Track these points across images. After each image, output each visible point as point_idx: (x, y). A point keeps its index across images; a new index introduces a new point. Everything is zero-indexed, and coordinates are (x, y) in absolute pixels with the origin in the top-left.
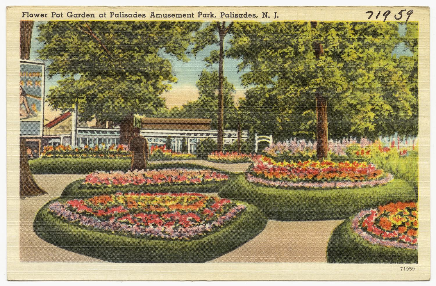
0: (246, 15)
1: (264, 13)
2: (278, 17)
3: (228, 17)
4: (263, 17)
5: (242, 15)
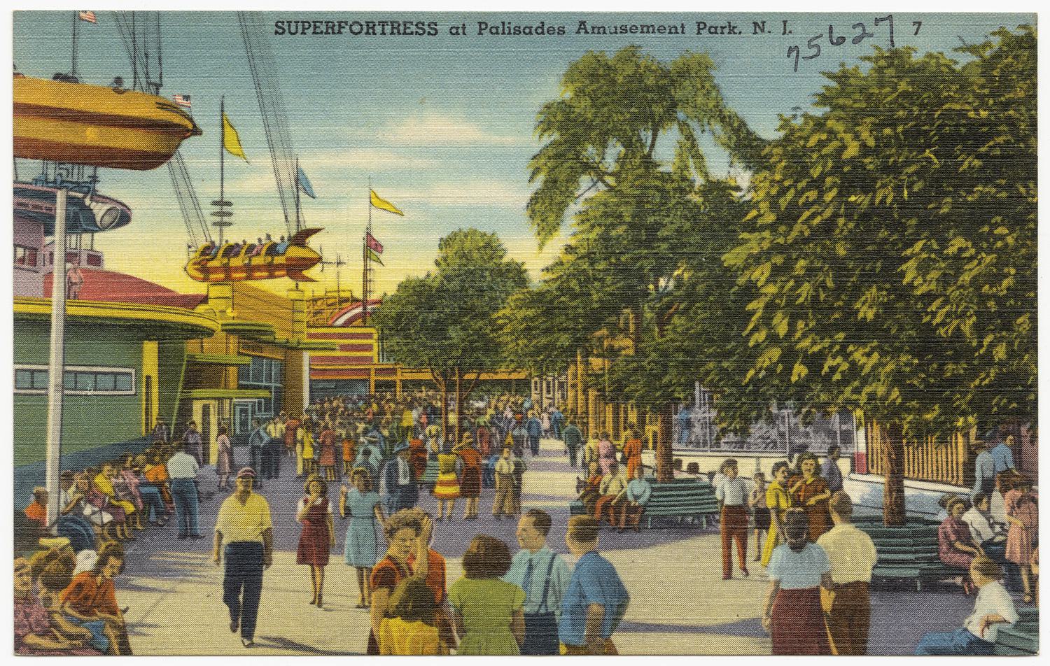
1: (756, 24)
2: (790, 32)
3: (497, 33)
4: (755, 33)
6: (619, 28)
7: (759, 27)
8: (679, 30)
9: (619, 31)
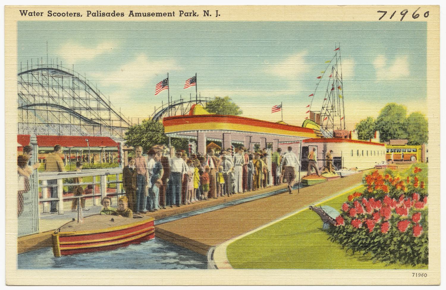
0: (114, 14)
1: (205, 11)
2: (219, 15)
3: (95, 16)
4: (205, 16)
5: (109, 14)
6: (147, 13)
7: (206, 13)
8: (172, 15)
9: (147, 15)
